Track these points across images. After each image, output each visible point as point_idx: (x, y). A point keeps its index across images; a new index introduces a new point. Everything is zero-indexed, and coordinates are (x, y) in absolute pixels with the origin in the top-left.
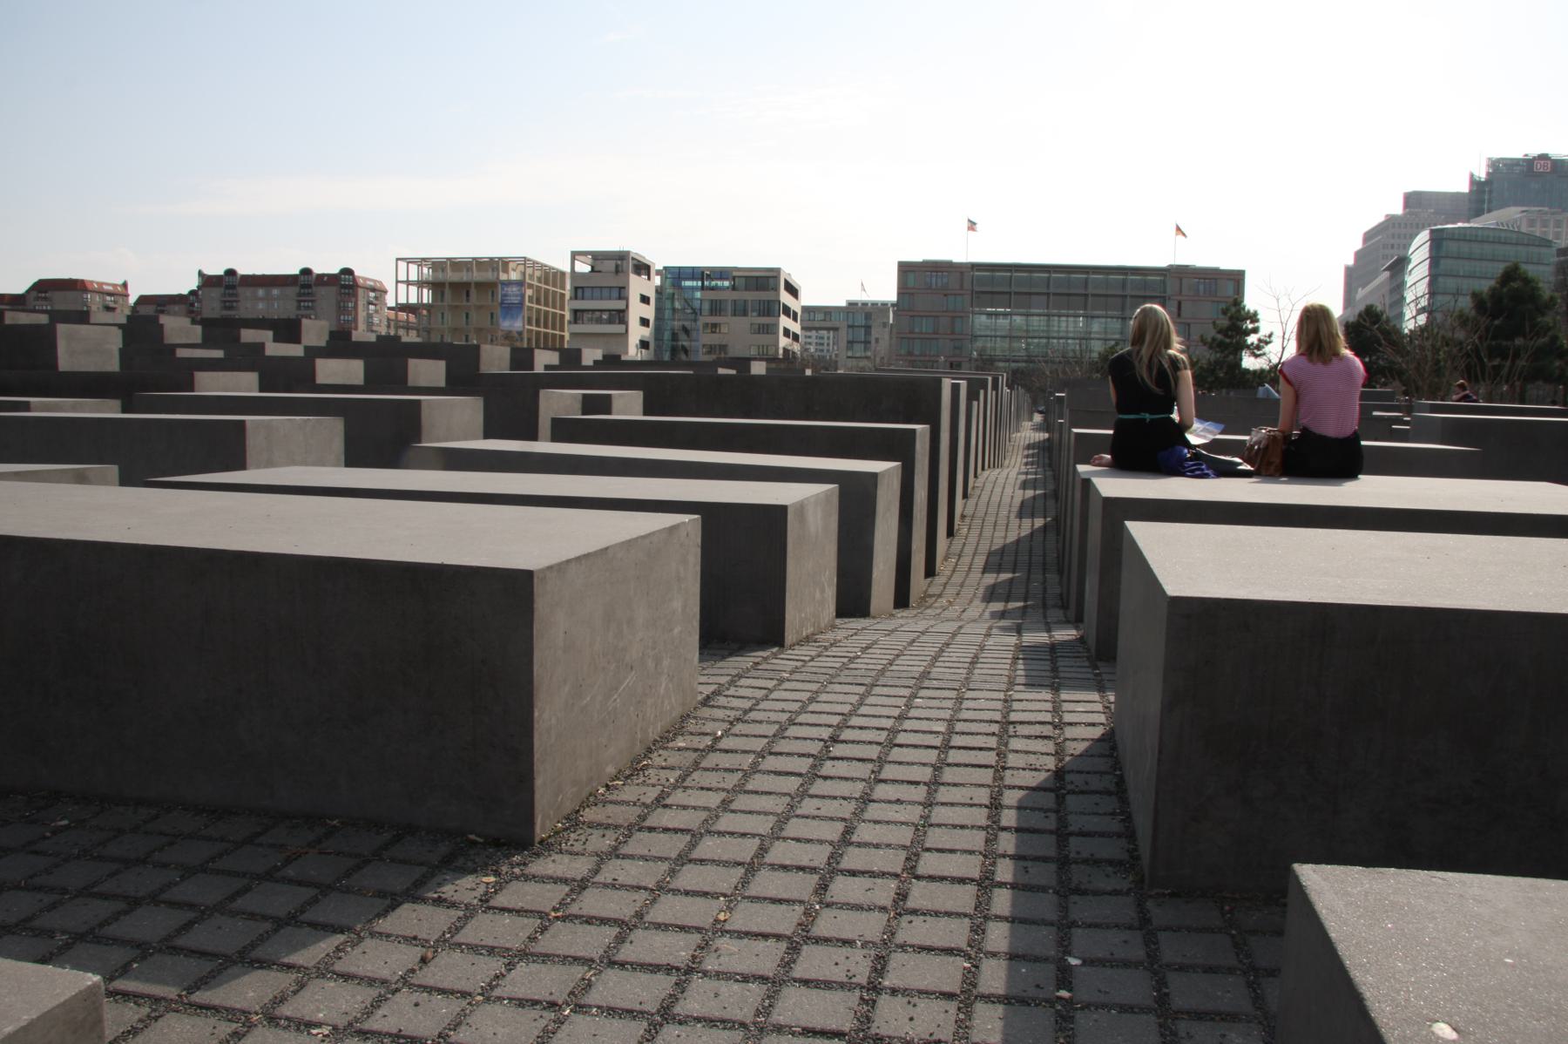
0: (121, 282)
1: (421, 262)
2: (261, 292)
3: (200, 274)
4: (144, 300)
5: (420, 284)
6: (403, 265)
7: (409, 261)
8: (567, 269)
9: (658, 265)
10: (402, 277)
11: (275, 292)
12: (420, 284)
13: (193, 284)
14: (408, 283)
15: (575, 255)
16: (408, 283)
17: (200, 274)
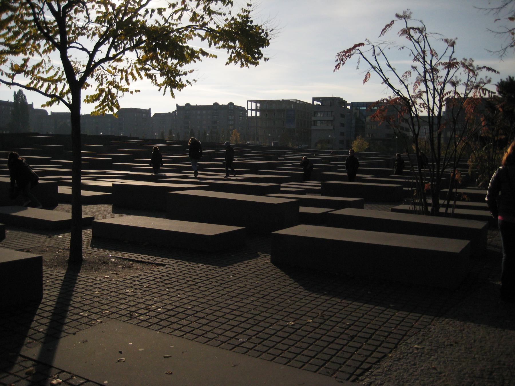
0: (148, 109)
1: (257, 102)
2: (199, 112)
3: (177, 105)
4: (156, 115)
5: (256, 110)
6: (250, 103)
7: (252, 101)
8: (311, 103)
9: (349, 102)
10: (250, 108)
11: (204, 112)
12: (256, 110)
13: (174, 109)
14: (252, 110)
15: (314, 99)
16: (252, 110)
17: (177, 105)
